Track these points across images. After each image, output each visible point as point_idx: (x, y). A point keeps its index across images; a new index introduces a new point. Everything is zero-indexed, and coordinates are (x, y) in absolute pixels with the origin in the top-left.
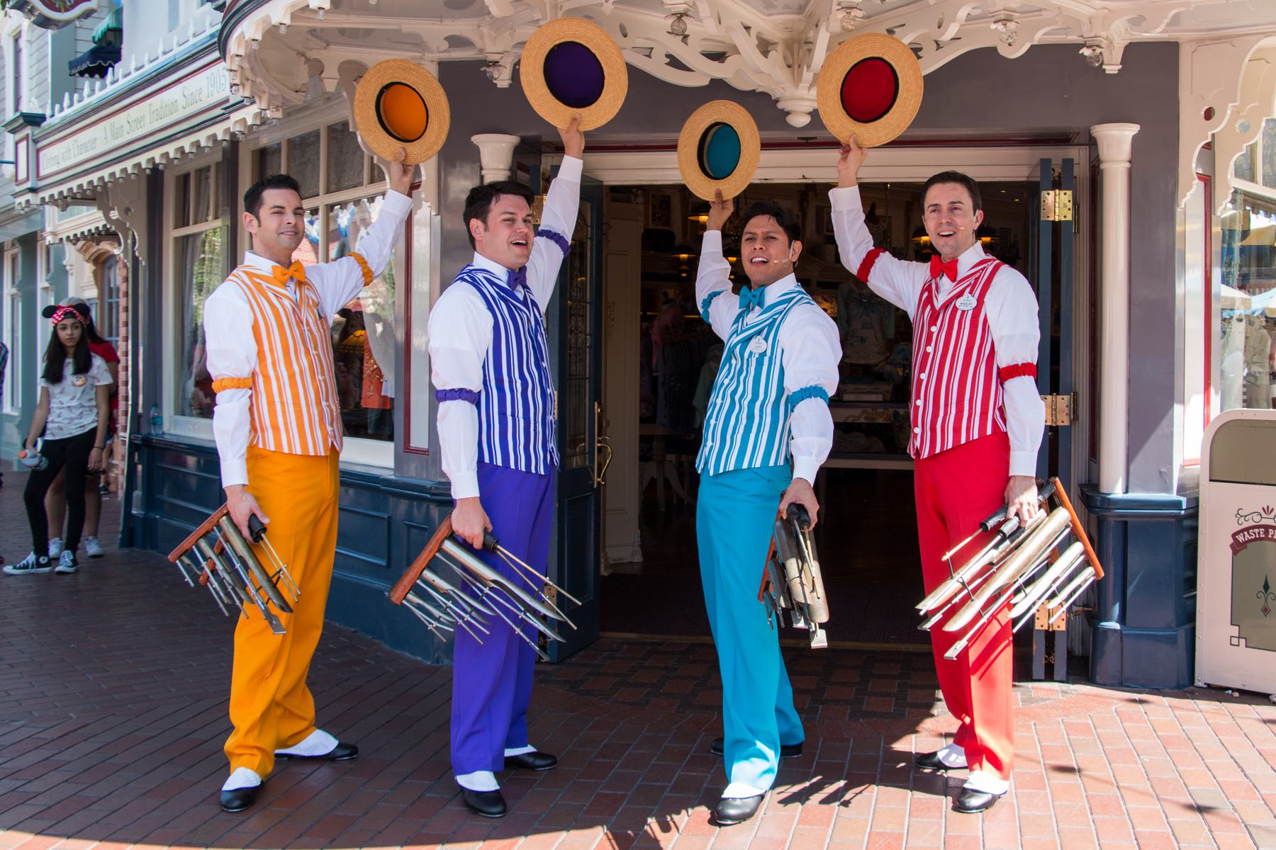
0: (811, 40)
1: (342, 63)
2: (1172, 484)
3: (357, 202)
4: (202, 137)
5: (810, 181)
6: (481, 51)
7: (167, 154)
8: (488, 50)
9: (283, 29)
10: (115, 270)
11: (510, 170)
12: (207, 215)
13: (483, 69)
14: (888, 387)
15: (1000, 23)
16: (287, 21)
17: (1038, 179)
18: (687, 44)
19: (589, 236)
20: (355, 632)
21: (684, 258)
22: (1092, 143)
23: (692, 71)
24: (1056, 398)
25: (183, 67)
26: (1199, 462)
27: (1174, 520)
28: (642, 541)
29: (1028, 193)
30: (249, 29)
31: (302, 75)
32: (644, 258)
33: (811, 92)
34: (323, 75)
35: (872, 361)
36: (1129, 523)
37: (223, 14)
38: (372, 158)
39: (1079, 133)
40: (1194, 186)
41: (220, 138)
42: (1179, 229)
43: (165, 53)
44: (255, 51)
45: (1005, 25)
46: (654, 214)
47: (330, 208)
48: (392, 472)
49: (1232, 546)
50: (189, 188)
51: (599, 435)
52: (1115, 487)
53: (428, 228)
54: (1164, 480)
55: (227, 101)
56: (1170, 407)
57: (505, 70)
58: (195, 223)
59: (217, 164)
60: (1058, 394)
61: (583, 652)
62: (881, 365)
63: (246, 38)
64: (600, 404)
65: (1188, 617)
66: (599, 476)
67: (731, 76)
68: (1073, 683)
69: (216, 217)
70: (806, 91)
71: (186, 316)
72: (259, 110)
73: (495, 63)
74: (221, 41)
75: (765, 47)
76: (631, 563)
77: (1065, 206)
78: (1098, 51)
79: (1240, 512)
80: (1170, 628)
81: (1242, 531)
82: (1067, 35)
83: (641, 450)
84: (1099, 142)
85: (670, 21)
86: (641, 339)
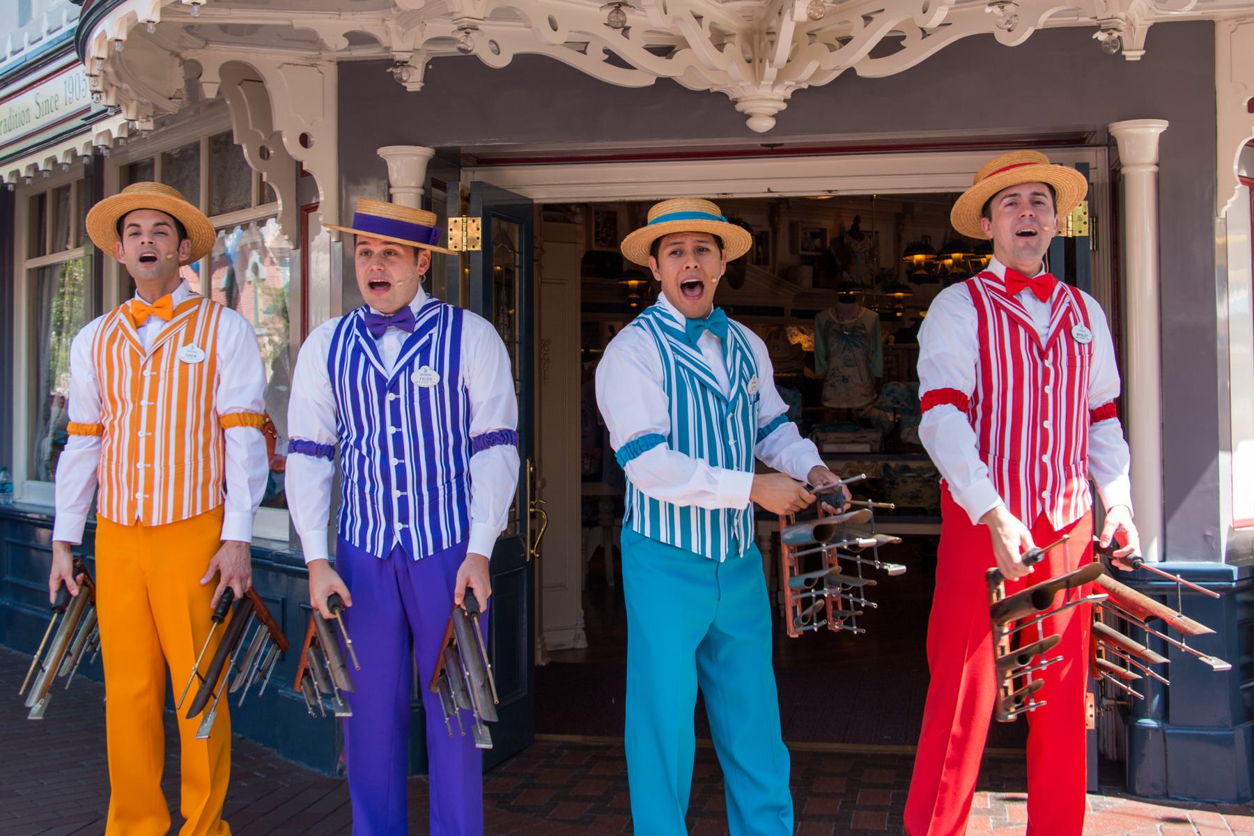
0: (774, 30)
1: (224, 65)
2: (1220, 551)
3: (245, 226)
4: (59, 152)
5: (776, 195)
6: (387, 49)
7: (17, 172)
8: (394, 50)
9: (151, 26)
11: (423, 187)
12: (67, 242)
13: (389, 70)
14: (876, 436)
15: (996, 6)
16: (156, 18)
18: (628, 38)
19: (517, 264)
20: (243, 738)
21: (633, 285)
22: (1111, 144)
23: (634, 68)
25: (37, 69)
28: (585, 623)
30: (111, 27)
31: (178, 81)
32: (584, 286)
33: (775, 91)
34: (201, 79)
35: (857, 405)
37: (81, 7)
38: (261, 175)
39: (1095, 132)
40: (1237, 192)
41: (80, 153)
42: (1219, 241)
43: (14, 53)
44: (119, 53)
45: (1003, 7)
46: (597, 234)
48: (287, 546)
50: (46, 211)
51: (533, 498)
53: (328, 256)
55: (88, 109)
56: (1215, 455)
57: (415, 70)
58: (53, 252)
59: (79, 182)
61: (515, 759)
62: (867, 409)
63: (108, 39)
64: (532, 462)
66: (532, 548)
67: (682, 74)
68: (1107, 795)
69: (78, 245)
70: (769, 90)
71: (41, 363)
72: (126, 121)
73: (403, 64)
74: (78, 42)
75: (720, 40)
76: (573, 649)
77: (1080, 219)
78: (1115, 35)
80: (1225, 727)
82: (1078, 16)
83: (584, 512)
85: (607, 12)
86: (582, 383)
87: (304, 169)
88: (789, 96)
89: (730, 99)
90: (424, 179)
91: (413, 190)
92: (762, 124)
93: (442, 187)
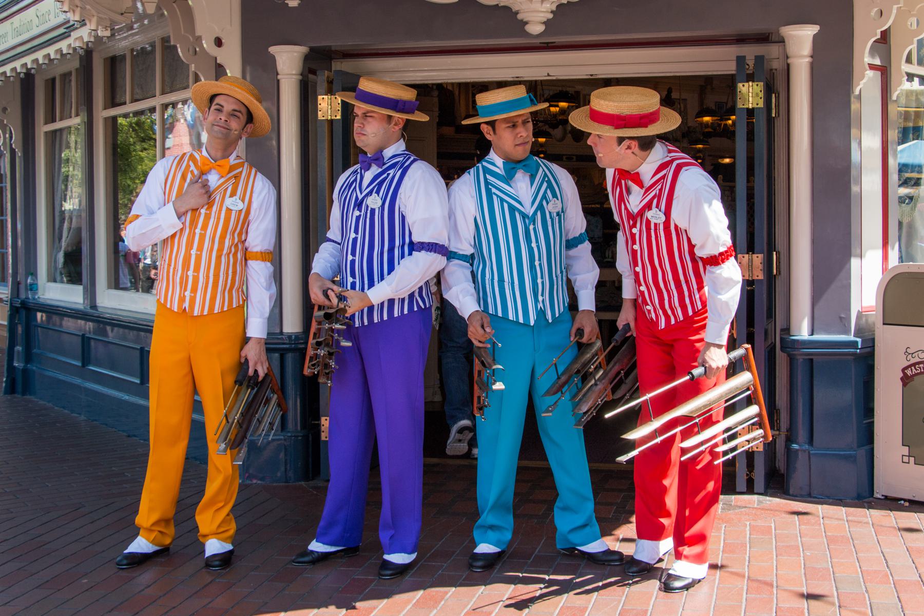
2: (851, 328)
10: (4, 159)
11: (301, 75)
17: (734, 72)
22: (782, 41)
24: (752, 257)
26: (874, 309)
27: (852, 357)
29: (729, 83)
33: (544, 5)
36: (814, 360)
47: (165, 107)
49: (902, 379)
52: (803, 331)
54: (843, 324)
55: (68, 22)
56: (848, 261)
60: (753, 253)
65: (868, 437)
70: (539, 5)
77: (757, 95)
79: (909, 351)
81: (910, 366)
84: (786, 40)
87: (218, 62)
88: (554, 8)
89: (513, 11)
90: (302, 68)
91: (294, 77)
92: (536, 29)
93: (313, 72)
